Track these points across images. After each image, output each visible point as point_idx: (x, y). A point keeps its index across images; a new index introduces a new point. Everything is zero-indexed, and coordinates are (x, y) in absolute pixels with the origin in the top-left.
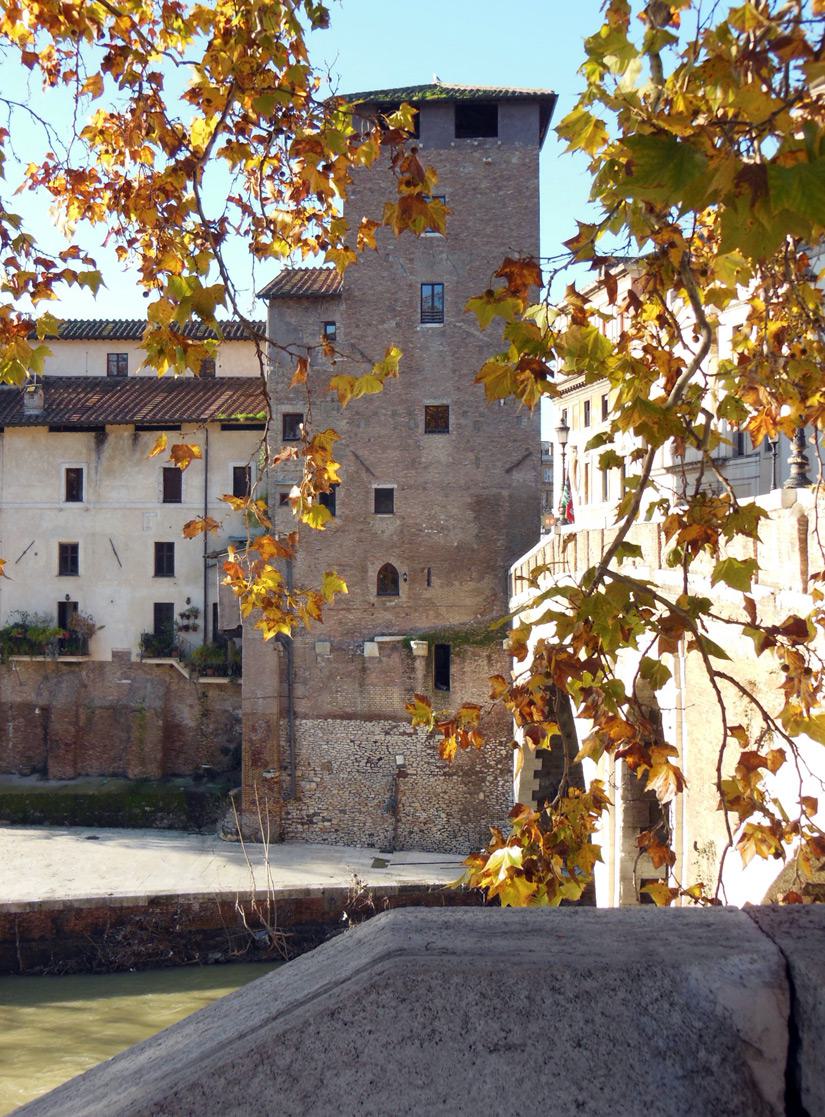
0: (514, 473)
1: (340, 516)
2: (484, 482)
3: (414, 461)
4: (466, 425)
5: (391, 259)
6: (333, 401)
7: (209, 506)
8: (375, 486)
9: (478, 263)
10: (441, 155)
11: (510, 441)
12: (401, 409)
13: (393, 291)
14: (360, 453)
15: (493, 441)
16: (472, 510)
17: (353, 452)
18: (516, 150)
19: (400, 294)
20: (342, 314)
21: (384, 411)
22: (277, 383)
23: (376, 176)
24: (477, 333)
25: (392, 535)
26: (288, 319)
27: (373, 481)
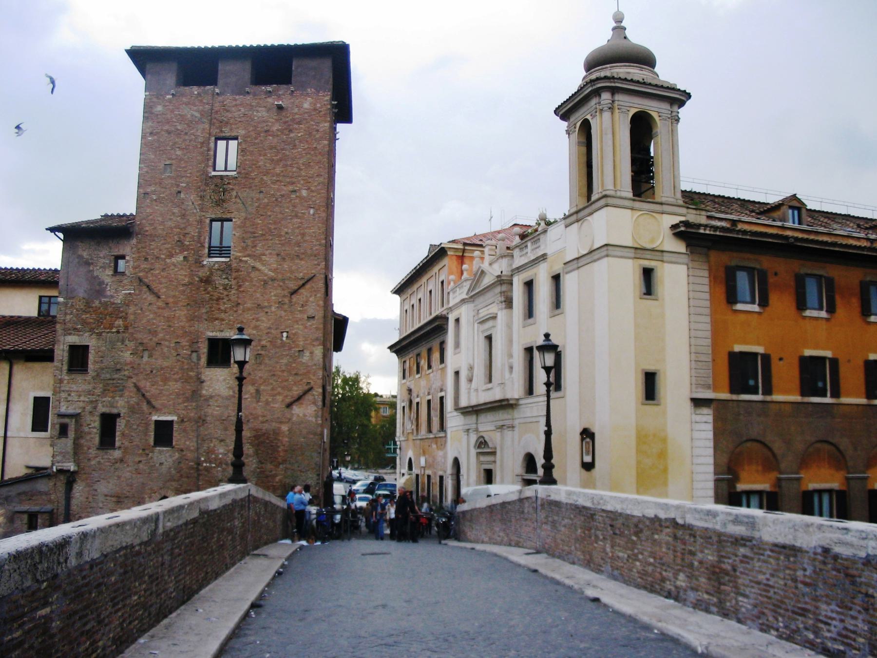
1: (120, 448)
2: (264, 416)
5: (182, 195)
6: (118, 332)
7: (9, 434)
8: (155, 418)
9: (266, 200)
10: (236, 100)
12: (184, 342)
13: (183, 226)
14: (142, 384)
15: (274, 375)
18: (309, 97)
19: (189, 229)
20: (132, 248)
21: (167, 343)
22: (66, 314)
23: (174, 120)
24: (263, 268)
25: (170, 468)
26: (80, 252)
27: (153, 413)
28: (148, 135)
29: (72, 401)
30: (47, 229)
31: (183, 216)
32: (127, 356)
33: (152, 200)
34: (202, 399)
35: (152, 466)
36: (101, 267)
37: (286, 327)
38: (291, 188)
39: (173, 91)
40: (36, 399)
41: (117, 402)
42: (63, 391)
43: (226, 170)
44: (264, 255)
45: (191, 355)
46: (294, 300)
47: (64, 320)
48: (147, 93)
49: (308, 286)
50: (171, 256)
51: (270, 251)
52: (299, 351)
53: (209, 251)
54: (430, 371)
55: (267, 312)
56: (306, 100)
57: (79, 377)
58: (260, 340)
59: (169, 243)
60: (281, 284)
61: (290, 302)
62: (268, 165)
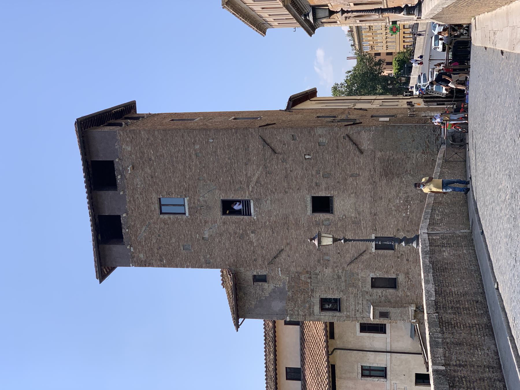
0: (362, 148)
2: (370, 170)
3: (353, 222)
4: (327, 183)
6: (310, 278)
7: (389, 349)
8: (373, 250)
9: (205, 175)
10: (130, 201)
11: (337, 152)
14: (348, 260)
15: (338, 164)
16: (392, 180)
17: (348, 265)
19: (231, 230)
22: (298, 315)
23: (149, 245)
24: (257, 175)
28: (162, 263)
29: (363, 308)
30: (237, 331)
31: (221, 235)
32: (328, 271)
34: (358, 216)
35: (410, 251)
36: (263, 292)
37: (300, 155)
38: (194, 157)
39: (128, 247)
40: (362, 331)
41: (362, 277)
42: (355, 315)
43: (184, 205)
44: (246, 175)
45: (325, 225)
46: (280, 150)
47: (303, 316)
48: (131, 265)
49: (269, 141)
50: (251, 243)
51: (243, 171)
52: (319, 145)
53: (246, 215)
54: (329, 5)
55: (291, 171)
56: (124, 149)
57: (344, 305)
58: (312, 175)
59: (242, 244)
60: (268, 161)
61: (281, 154)
62: (178, 175)
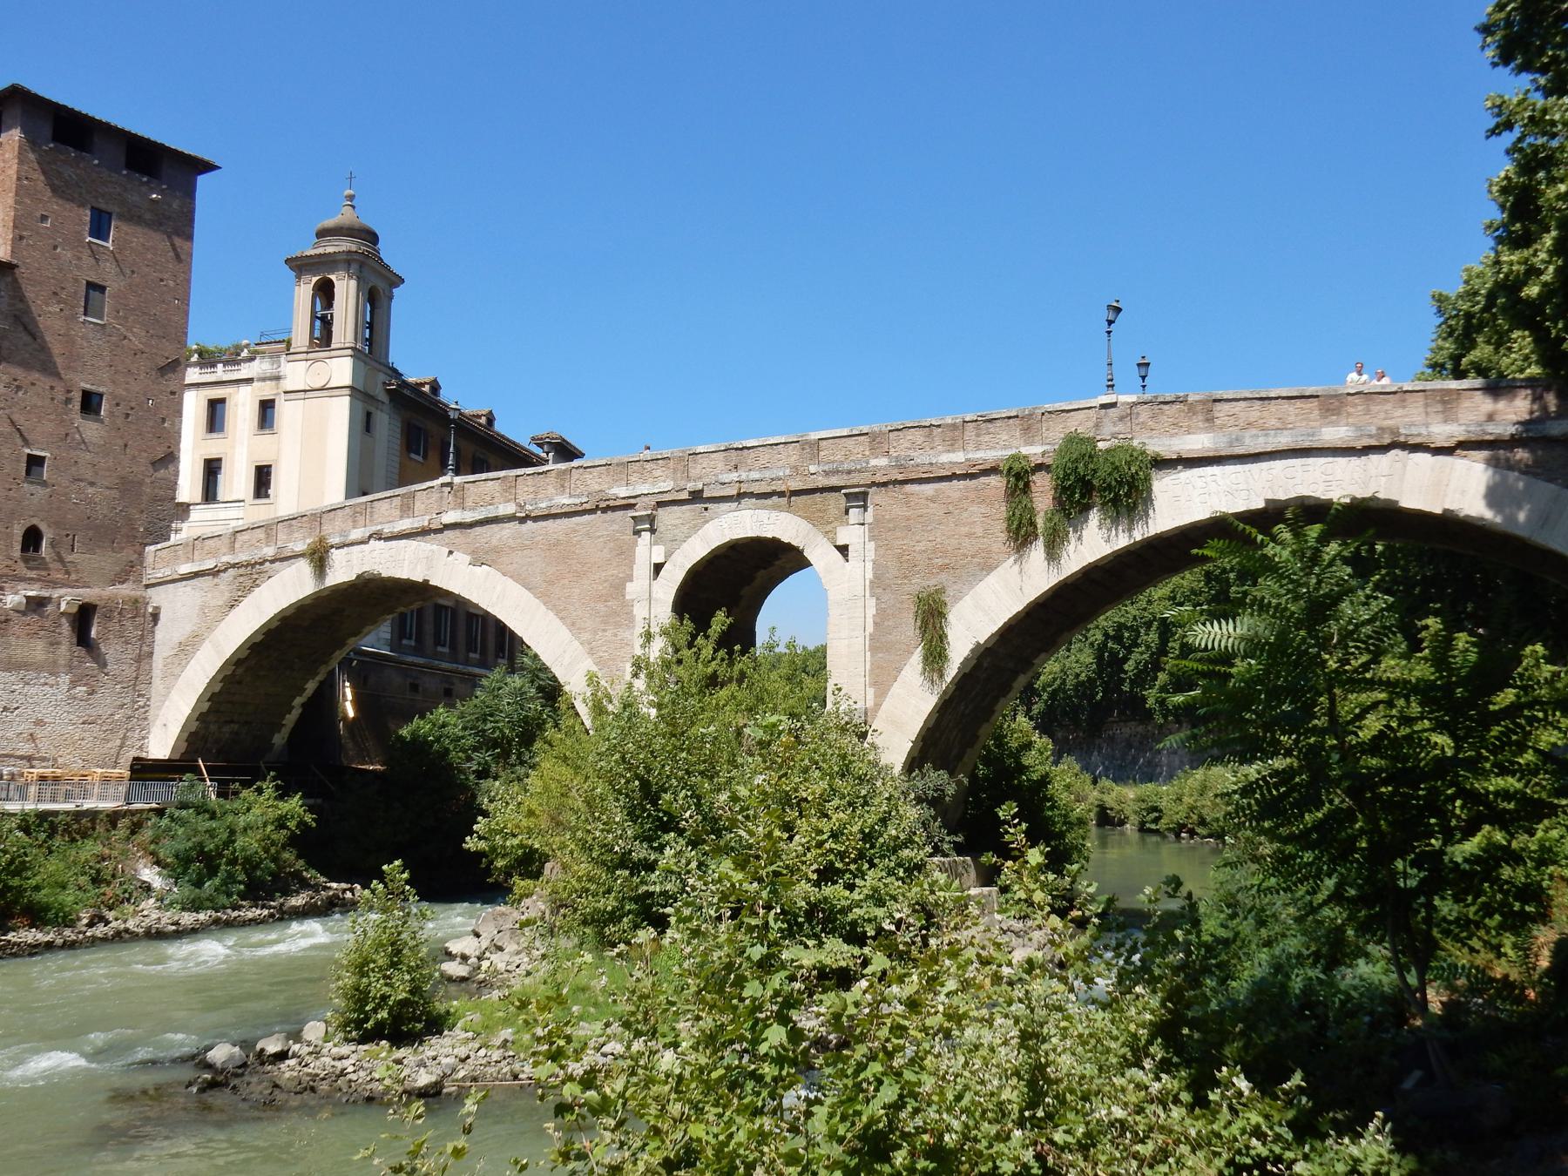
8: (28, 451)
14: (15, 417)
33: (28, 245)
50: (47, 305)
